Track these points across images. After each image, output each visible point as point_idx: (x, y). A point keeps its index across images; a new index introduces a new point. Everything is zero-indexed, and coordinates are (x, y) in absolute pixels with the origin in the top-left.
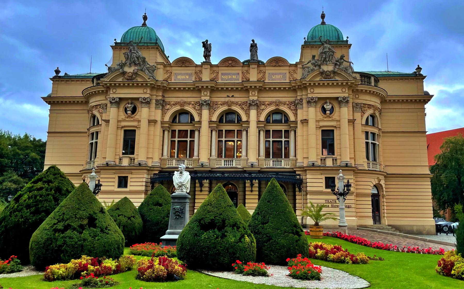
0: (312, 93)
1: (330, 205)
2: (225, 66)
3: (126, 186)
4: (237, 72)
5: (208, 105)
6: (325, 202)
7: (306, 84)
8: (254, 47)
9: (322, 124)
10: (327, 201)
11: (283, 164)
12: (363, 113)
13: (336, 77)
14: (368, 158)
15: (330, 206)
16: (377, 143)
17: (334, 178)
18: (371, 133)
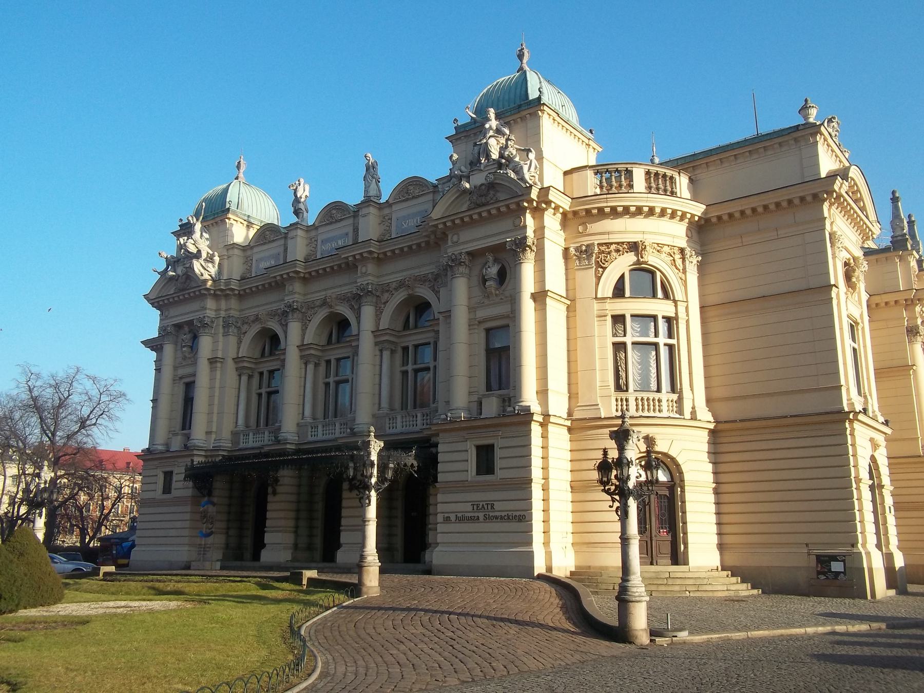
0: (456, 243)
1: (481, 515)
2: (328, 224)
3: (170, 492)
4: (345, 230)
5: (294, 310)
6: (470, 509)
7: (436, 226)
8: (371, 169)
9: (481, 314)
10: (476, 506)
11: (399, 425)
12: (601, 267)
13: (499, 195)
14: (620, 386)
15: (481, 518)
16: (662, 340)
17: (492, 446)
18: (632, 316)
